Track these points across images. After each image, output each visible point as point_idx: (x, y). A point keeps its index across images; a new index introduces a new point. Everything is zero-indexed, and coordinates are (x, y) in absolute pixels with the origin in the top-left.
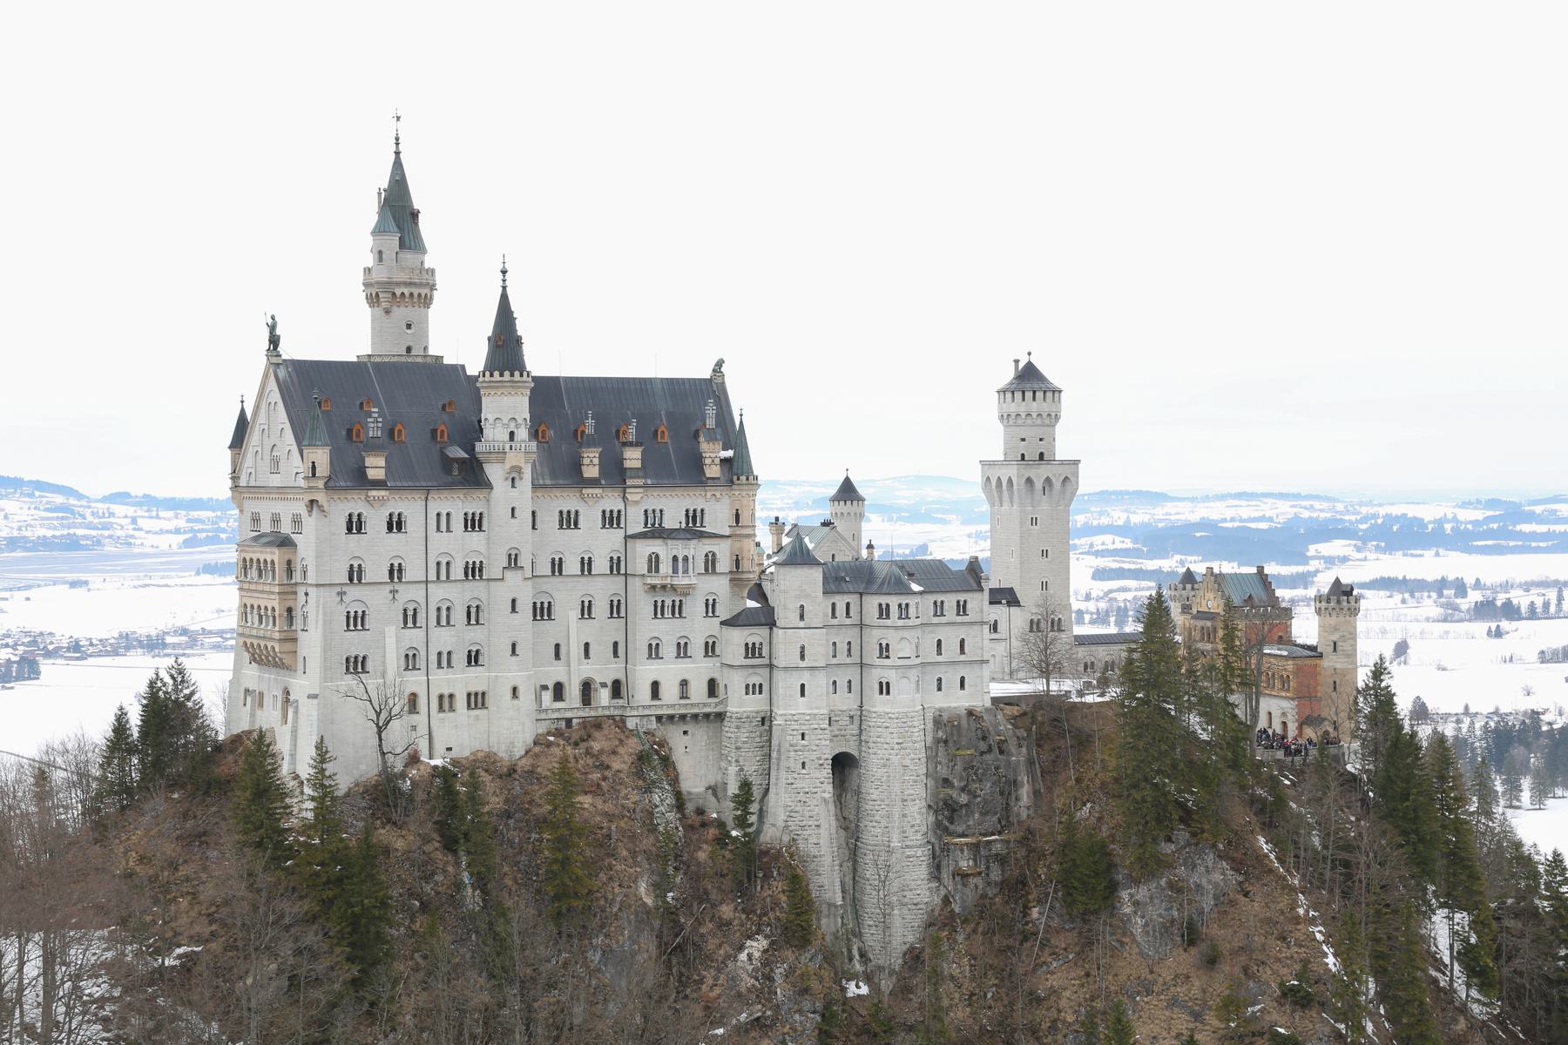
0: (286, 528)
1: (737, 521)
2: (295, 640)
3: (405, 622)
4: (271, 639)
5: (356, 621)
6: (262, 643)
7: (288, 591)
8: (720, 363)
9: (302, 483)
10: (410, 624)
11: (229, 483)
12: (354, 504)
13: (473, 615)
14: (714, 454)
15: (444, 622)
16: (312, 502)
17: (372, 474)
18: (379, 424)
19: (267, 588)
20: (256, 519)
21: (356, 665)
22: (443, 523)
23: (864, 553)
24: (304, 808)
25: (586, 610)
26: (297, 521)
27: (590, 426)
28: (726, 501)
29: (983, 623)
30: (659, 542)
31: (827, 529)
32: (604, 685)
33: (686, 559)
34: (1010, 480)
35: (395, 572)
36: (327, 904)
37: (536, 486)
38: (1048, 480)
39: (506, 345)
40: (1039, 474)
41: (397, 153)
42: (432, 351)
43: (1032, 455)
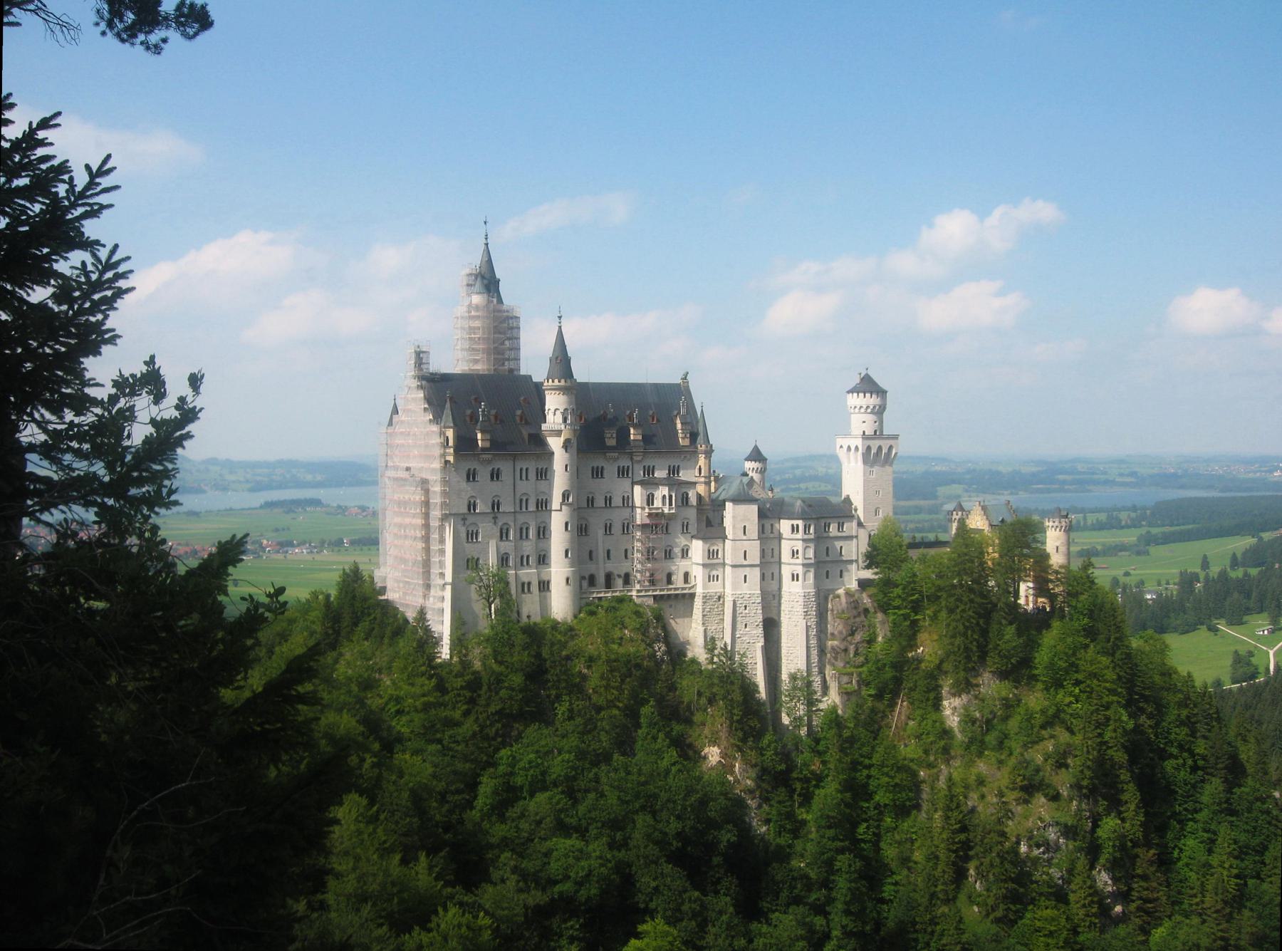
5: (472, 536)
12: (473, 465)
13: (543, 532)
22: (524, 474)
24: (445, 652)
25: (608, 529)
29: (850, 538)
31: (745, 480)
32: (619, 576)
33: (671, 497)
34: (857, 448)
35: (496, 505)
36: (466, 714)
37: (581, 451)
38: (880, 448)
40: (875, 444)
43: (869, 432)
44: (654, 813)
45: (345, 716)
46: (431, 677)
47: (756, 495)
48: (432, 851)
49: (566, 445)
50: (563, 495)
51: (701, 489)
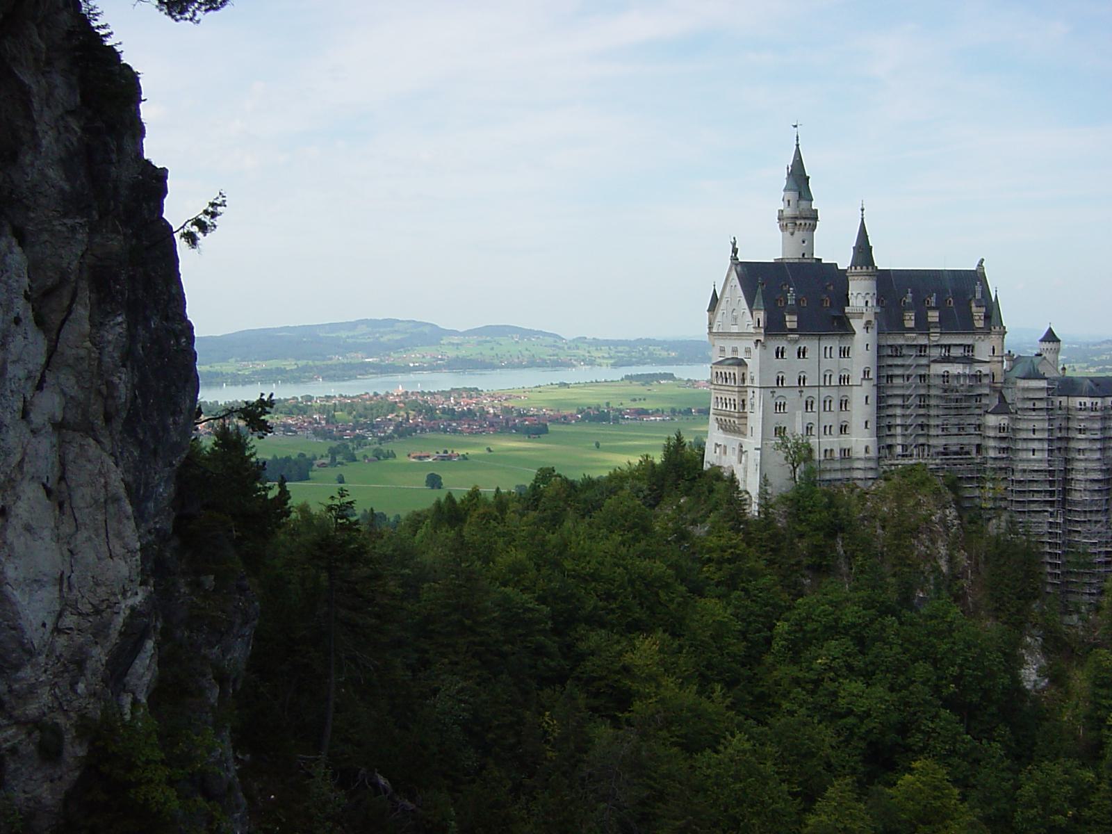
0: (741, 355)
1: (994, 353)
2: (746, 418)
3: (807, 408)
4: (735, 417)
5: (780, 407)
6: (727, 419)
7: (743, 390)
8: (982, 261)
9: (752, 331)
10: (809, 410)
11: (708, 330)
12: (781, 343)
13: (844, 404)
14: (978, 313)
15: (827, 409)
16: (757, 341)
17: (789, 325)
18: (794, 295)
19: (730, 389)
20: (722, 350)
21: (780, 431)
22: (828, 352)
23: (1061, 372)
24: (754, 509)
26: (748, 351)
27: (909, 298)
28: (987, 341)
30: (950, 364)
31: (1040, 358)
36: (771, 563)
37: (880, 332)
39: (863, 250)
41: (798, 145)
42: (815, 256)
44: (935, 663)
45: (658, 562)
46: (738, 531)
47: (1046, 376)
48: (730, 684)
49: (867, 325)
50: (865, 372)
51: (996, 368)
